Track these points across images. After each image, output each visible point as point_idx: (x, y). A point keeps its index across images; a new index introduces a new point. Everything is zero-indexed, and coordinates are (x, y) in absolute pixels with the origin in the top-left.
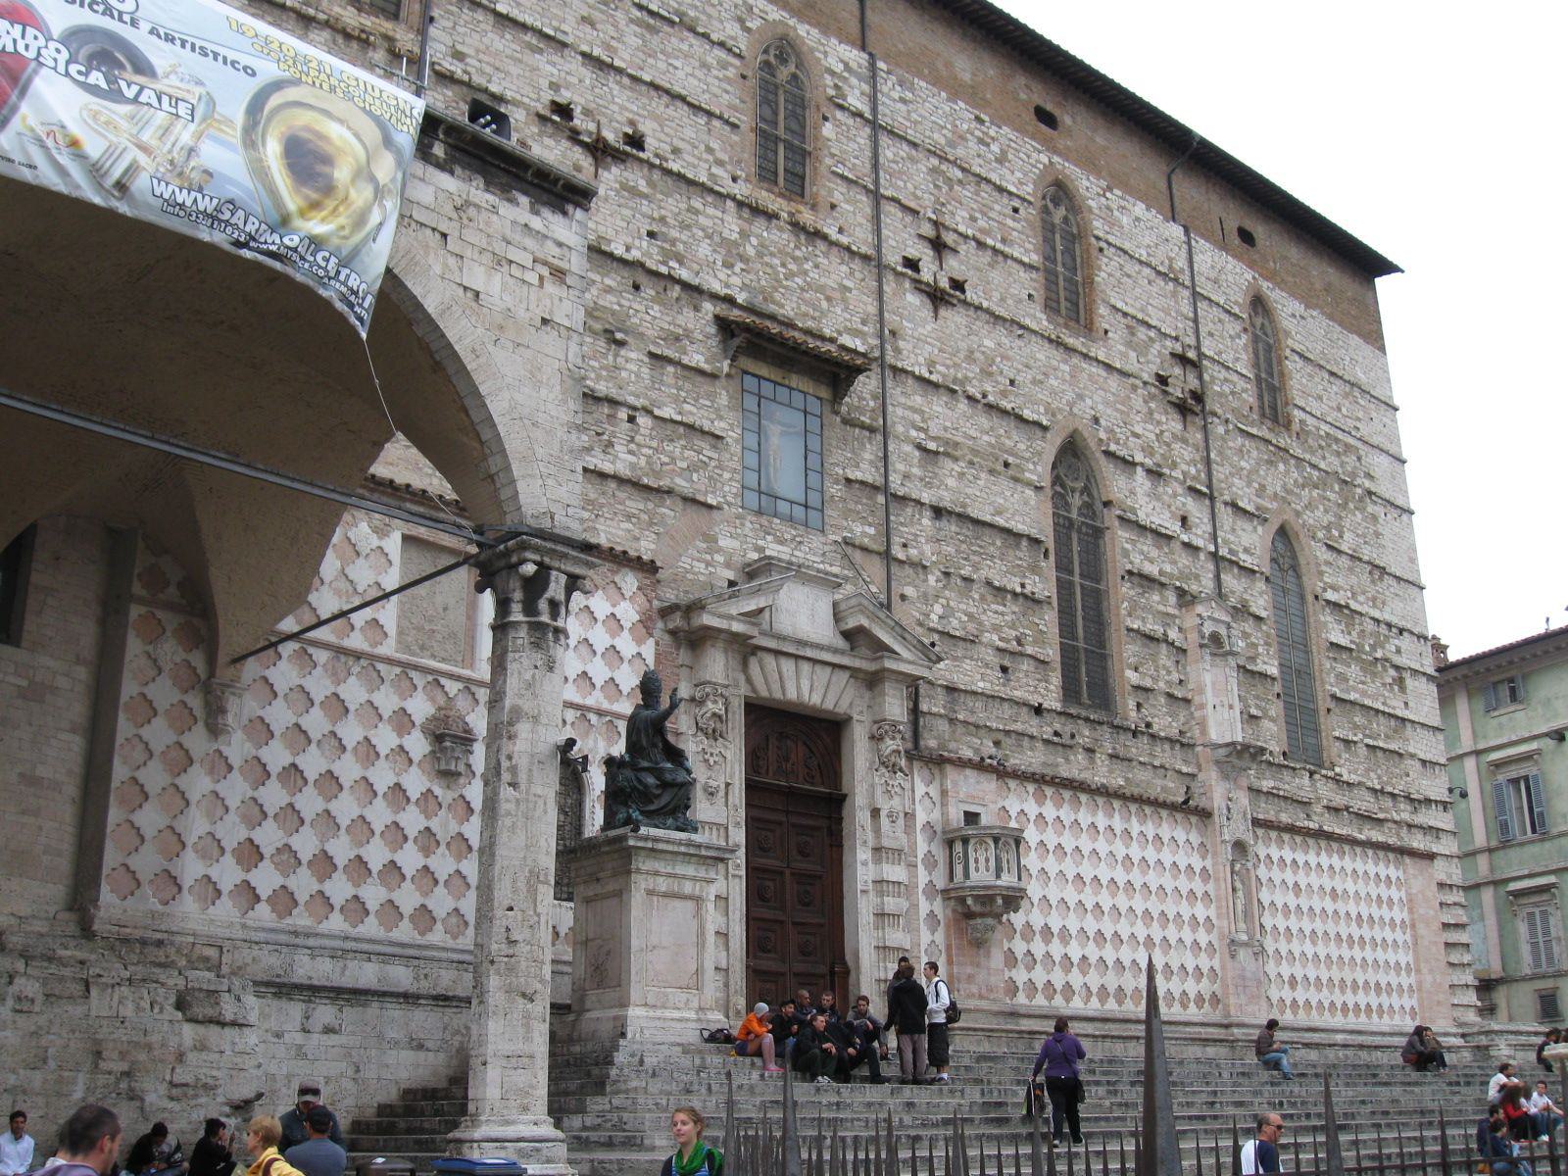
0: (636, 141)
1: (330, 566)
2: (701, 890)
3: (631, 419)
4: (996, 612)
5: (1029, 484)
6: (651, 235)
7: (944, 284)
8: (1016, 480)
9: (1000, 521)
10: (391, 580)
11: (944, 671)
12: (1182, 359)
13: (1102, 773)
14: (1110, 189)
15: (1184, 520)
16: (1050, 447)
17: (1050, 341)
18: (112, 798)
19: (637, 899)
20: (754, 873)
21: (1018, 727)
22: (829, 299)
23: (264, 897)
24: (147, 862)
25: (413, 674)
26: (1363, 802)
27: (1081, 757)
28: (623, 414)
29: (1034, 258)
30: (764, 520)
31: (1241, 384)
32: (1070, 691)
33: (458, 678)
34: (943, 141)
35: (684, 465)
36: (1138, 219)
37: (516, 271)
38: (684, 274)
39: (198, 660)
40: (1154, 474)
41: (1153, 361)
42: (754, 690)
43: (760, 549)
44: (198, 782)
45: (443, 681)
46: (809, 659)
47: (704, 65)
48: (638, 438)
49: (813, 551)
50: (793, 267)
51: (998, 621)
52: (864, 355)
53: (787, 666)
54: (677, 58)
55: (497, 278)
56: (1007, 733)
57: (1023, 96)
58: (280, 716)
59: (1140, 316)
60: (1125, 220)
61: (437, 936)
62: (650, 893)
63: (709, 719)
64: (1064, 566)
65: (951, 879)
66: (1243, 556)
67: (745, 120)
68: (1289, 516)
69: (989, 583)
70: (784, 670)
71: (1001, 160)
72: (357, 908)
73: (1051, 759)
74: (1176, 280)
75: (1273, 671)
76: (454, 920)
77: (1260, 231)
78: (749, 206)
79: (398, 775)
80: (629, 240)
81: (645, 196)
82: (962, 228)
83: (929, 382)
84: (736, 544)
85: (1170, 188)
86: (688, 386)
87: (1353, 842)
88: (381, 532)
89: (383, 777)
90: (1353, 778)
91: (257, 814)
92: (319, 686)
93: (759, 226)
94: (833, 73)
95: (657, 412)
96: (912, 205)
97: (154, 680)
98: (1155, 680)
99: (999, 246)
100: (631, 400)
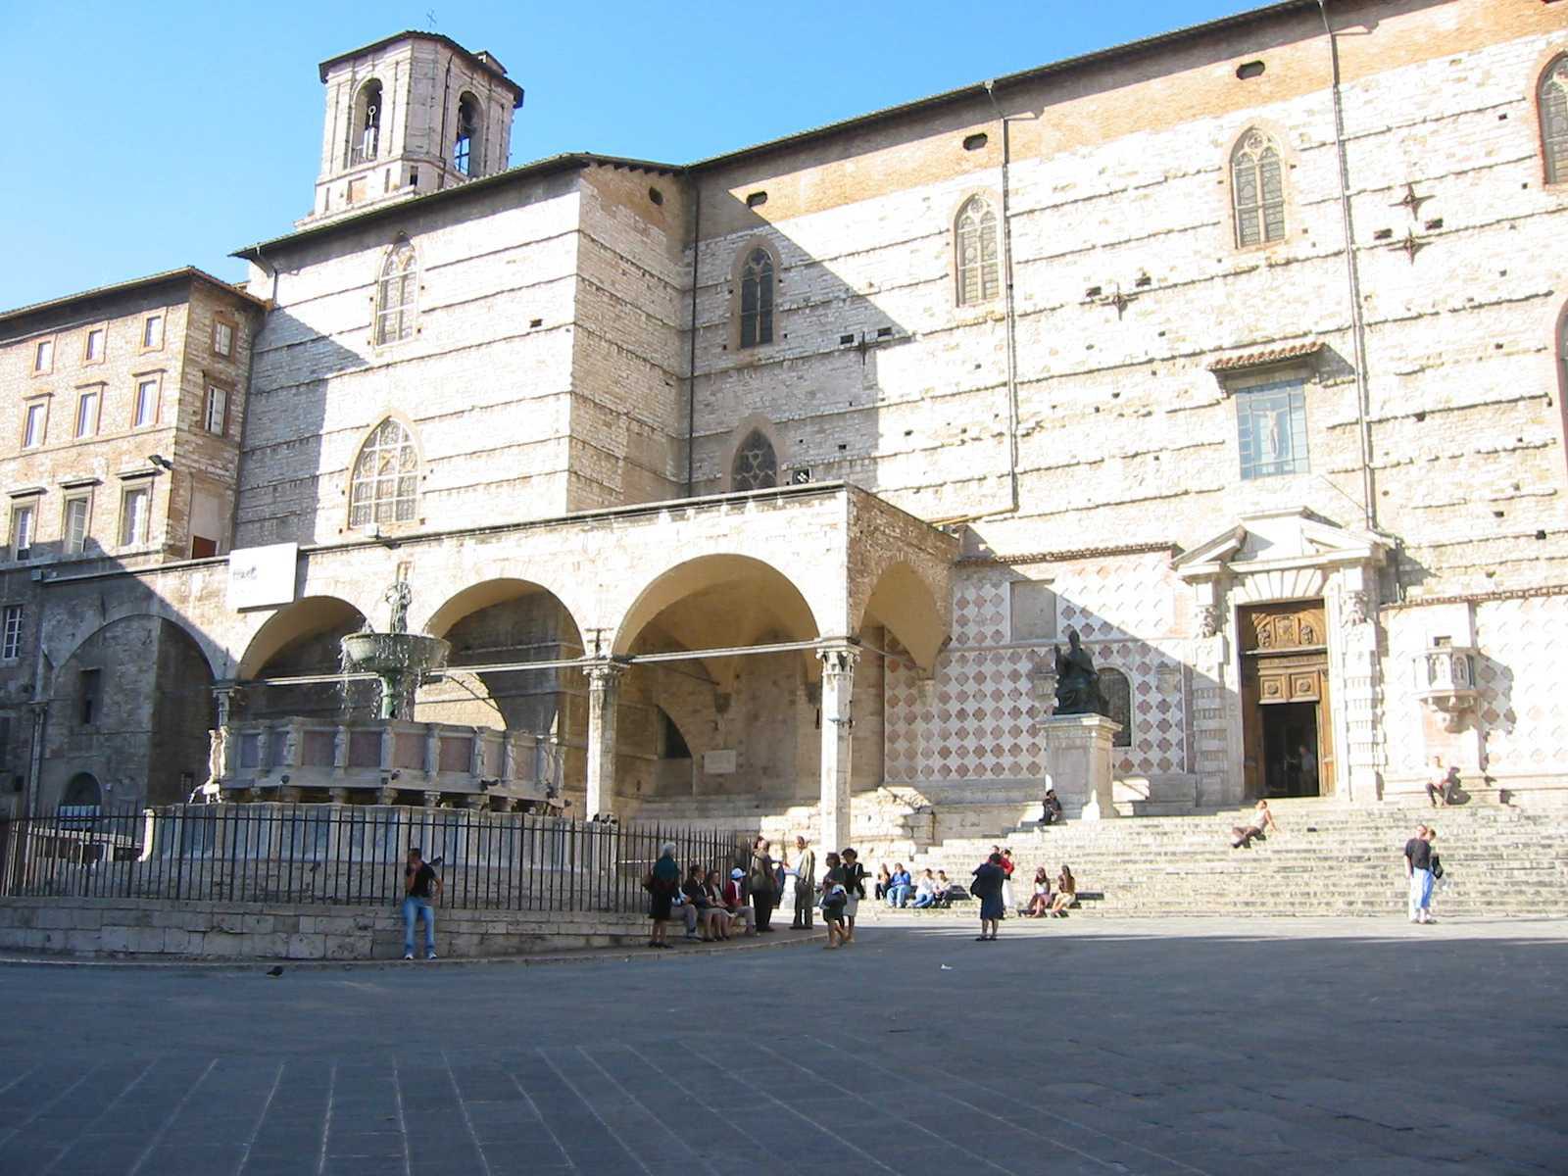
0: (1145, 281)
4: (1488, 472)
5: (1526, 351)
7: (1419, 230)
8: (1509, 354)
22: (1306, 303)
28: (1150, 457)
44: (920, 726)
45: (1036, 649)
49: (1300, 490)
58: (953, 688)
67: (1224, 214)
72: (998, 769)
73: (1557, 572)
81: (1153, 312)
88: (996, 586)
89: (1006, 705)
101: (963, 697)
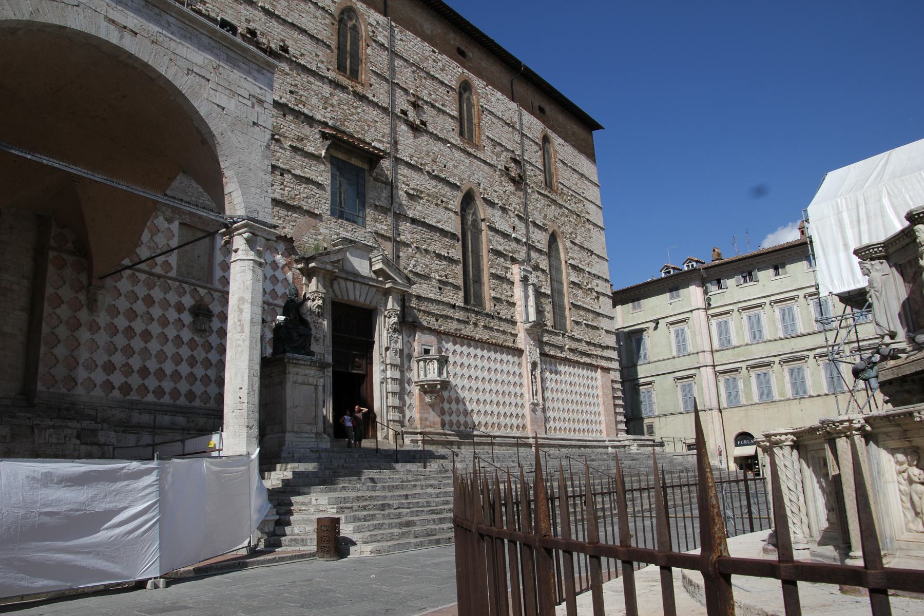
0: (285, 49)
1: (146, 236)
2: (317, 381)
3: (282, 175)
6: (291, 92)
7: (418, 122)
8: (447, 209)
9: (439, 225)
10: (174, 243)
11: (415, 290)
12: (515, 161)
13: (480, 334)
14: (487, 85)
15: (514, 228)
16: (459, 196)
17: (461, 150)
18: (42, 343)
19: (289, 385)
20: (334, 372)
21: (445, 313)
22: (368, 126)
23: (117, 386)
24: (60, 371)
25: (184, 285)
26: (583, 347)
27: (471, 326)
29: (455, 113)
30: (340, 221)
31: (538, 172)
32: (466, 300)
33: (205, 288)
34: (418, 59)
35: (305, 196)
36: (498, 99)
37: (241, 99)
38: (306, 111)
39: (83, 278)
40: (504, 209)
41: (502, 161)
42: (336, 295)
43: (338, 234)
45: (198, 289)
46: (359, 282)
47: (316, 17)
48: (285, 183)
50: (353, 110)
51: (437, 269)
52: (382, 151)
53: (350, 285)
54: (303, 13)
55: (233, 101)
56: (442, 316)
57: (452, 42)
58: (122, 304)
59: (498, 141)
60: (493, 99)
61: (197, 403)
62: (295, 382)
63: (317, 307)
64: (464, 246)
65: (419, 377)
66: (537, 244)
67: (334, 44)
68: (556, 228)
69: (434, 252)
70: (348, 286)
71: (442, 70)
72: (160, 392)
74: (513, 127)
75: (549, 292)
76: (205, 396)
77: (548, 108)
78: (334, 82)
79: (178, 331)
80: (281, 94)
81: (288, 74)
82: (425, 98)
83: (410, 164)
84: (327, 231)
85: (512, 87)
86: (307, 160)
87: (578, 362)
89: (171, 332)
90: (579, 337)
91: (112, 349)
92: (141, 291)
93: (337, 92)
94: (372, 25)
95: (293, 172)
96: (404, 86)
97: (61, 287)
98: (501, 294)
99: (440, 107)
100: (281, 166)
101: (132, 315)
